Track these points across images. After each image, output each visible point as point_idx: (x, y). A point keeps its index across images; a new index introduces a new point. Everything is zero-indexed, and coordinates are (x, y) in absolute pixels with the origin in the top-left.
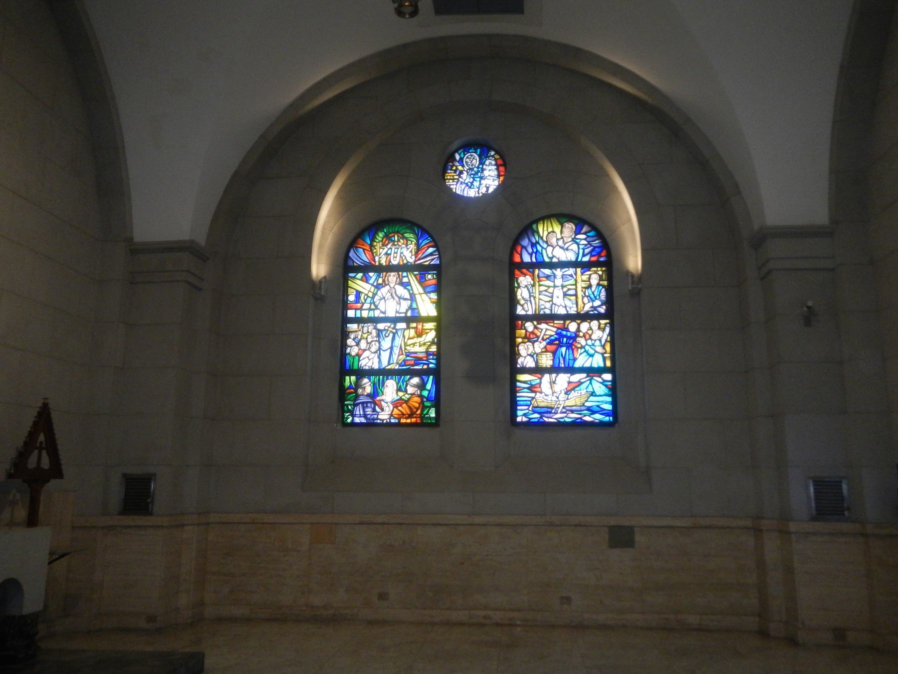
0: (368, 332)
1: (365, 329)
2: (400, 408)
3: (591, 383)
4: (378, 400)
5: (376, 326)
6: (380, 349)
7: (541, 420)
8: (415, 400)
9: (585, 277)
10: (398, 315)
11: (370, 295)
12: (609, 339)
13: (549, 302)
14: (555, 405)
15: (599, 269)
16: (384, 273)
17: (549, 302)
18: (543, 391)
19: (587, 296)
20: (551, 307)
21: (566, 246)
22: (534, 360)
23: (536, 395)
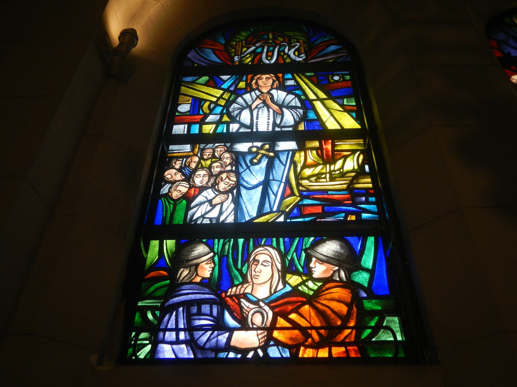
0: (214, 156)
1: (208, 153)
2: (293, 316)
4: (231, 297)
5: (231, 147)
6: (238, 185)
8: (336, 296)
10: (277, 129)
11: (222, 102)
16: (250, 77)
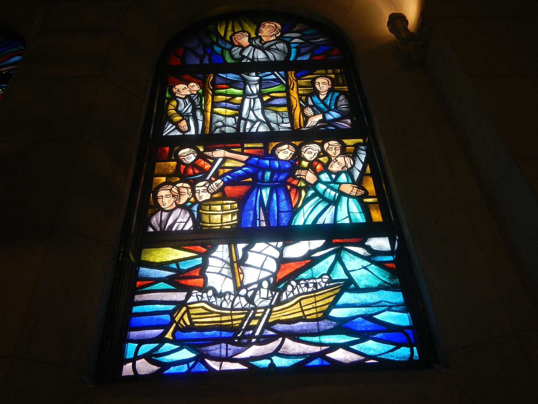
3: (339, 259)
7: (201, 368)
9: (302, 82)
12: (368, 170)
13: (233, 116)
14: (244, 320)
15: (330, 71)
17: (233, 116)
18: (210, 283)
19: (311, 107)
20: (238, 123)
21: (266, 46)
22: (192, 215)
23: (188, 297)
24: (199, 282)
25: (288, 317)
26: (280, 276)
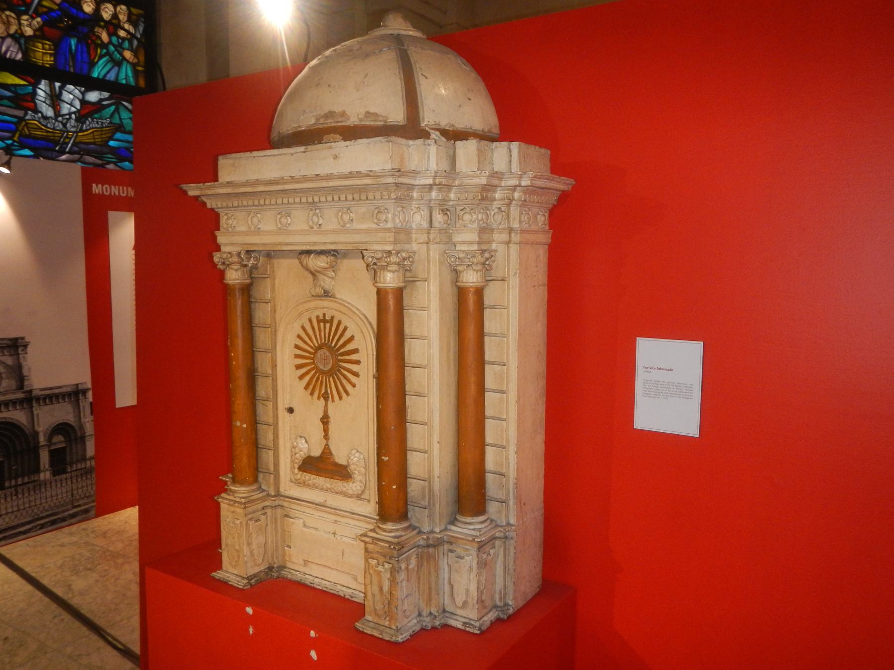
14: (61, 137)
23: (26, 114)
24: (31, 105)
25: (87, 141)
26: (84, 112)
